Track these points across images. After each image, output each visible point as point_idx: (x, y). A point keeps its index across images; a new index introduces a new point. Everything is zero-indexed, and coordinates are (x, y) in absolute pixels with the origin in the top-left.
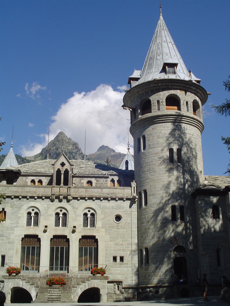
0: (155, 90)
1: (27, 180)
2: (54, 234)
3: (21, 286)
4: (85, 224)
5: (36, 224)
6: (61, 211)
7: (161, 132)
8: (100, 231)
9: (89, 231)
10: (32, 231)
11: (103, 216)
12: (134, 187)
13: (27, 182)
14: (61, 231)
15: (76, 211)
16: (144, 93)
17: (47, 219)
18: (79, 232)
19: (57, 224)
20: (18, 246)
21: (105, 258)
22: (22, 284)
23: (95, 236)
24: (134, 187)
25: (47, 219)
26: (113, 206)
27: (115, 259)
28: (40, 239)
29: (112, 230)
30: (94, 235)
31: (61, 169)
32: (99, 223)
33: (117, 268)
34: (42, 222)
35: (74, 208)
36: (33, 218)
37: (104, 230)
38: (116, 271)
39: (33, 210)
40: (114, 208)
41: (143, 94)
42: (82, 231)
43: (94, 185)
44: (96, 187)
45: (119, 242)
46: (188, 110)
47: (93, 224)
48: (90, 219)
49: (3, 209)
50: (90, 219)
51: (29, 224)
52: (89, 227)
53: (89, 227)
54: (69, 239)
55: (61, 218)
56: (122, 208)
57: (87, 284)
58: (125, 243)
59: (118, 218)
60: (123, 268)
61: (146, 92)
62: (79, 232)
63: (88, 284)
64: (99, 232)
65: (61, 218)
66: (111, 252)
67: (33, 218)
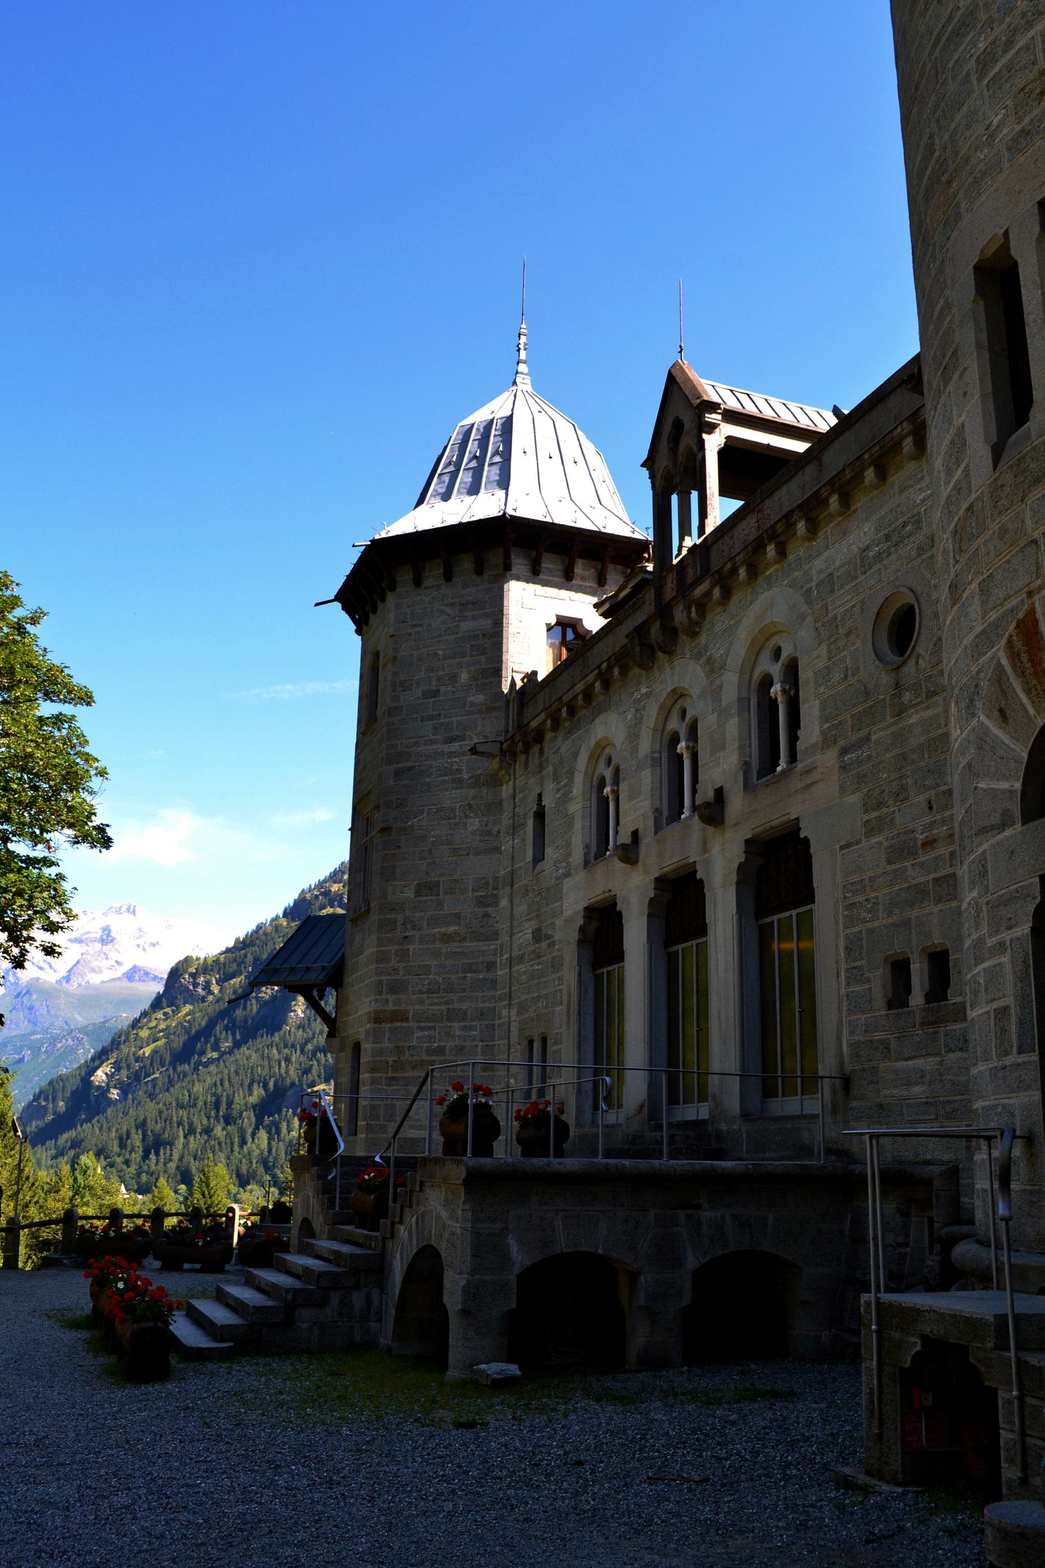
8: (816, 776)
11: (824, 649)
15: (720, 688)
18: (736, 825)
21: (848, 984)
26: (867, 548)
29: (868, 738)
33: (910, 1063)
35: (712, 671)
37: (829, 758)
38: (909, 1084)
40: (871, 554)
45: (914, 820)
56: (909, 528)
58: (943, 821)
60: (951, 1055)
62: (736, 825)
64: (814, 783)
66: (876, 924)
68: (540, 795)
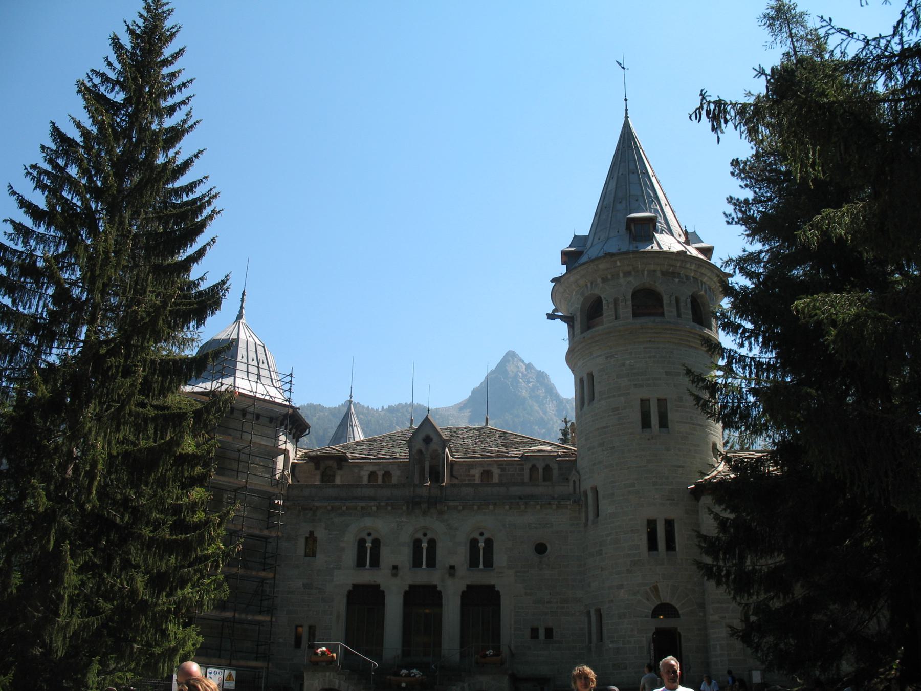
0: (609, 277)
1: (362, 473)
2: (411, 583)
3: (336, 687)
4: (473, 563)
5: (375, 563)
6: (425, 535)
7: (624, 365)
9: (480, 577)
10: (367, 577)
12: (574, 481)
13: (361, 477)
14: (423, 577)
16: (589, 285)
17: (396, 554)
19: (417, 563)
20: (340, 605)
22: (339, 683)
23: (493, 586)
24: (574, 481)
25: (396, 554)
27: (534, 632)
28: (383, 592)
30: (493, 583)
31: (423, 450)
32: (500, 558)
34: (387, 557)
36: (369, 553)
39: (369, 535)
41: (586, 285)
42: (466, 577)
43: (496, 479)
44: (500, 484)
46: (679, 315)
47: (489, 563)
48: (481, 553)
49: (312, 533)
50: (481, 553)
51: (360, 563)
52: (481, 566)
53: (481, 566)
54: (440, 592)
55: (424, 553)
57: (466, 685)
59: (541, 549)
61: (592, 283)
63: (469, 685)
65: (424, 553)
67: (369, 553)
68: (312, 533)
